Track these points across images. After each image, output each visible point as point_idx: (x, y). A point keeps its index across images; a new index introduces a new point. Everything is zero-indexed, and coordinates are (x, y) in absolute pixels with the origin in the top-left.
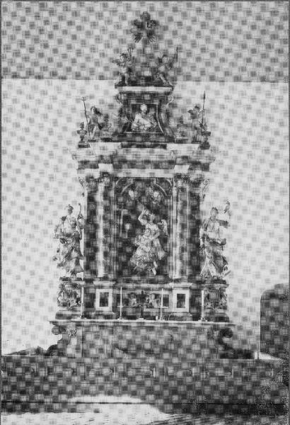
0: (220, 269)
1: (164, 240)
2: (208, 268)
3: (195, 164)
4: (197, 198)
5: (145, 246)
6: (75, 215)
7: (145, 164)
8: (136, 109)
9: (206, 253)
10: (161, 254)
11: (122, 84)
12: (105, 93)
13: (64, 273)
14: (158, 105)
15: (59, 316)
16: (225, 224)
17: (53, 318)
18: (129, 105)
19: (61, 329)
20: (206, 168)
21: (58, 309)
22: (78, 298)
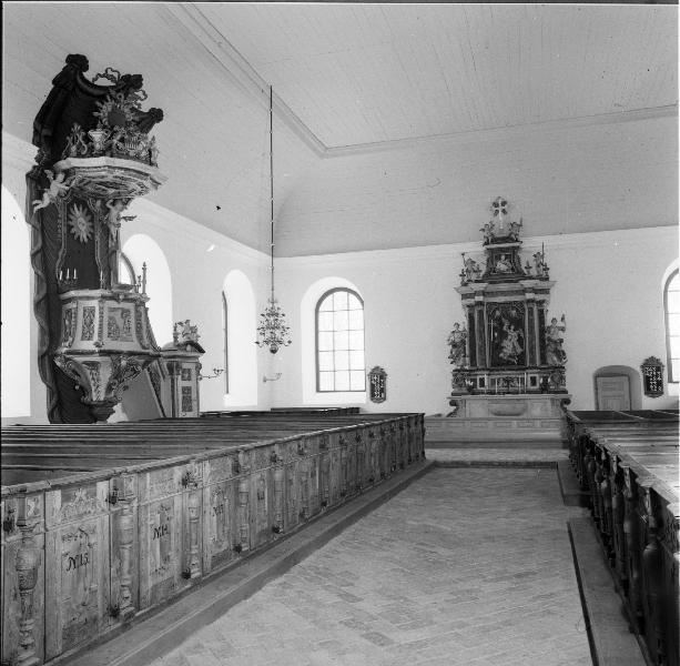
0: (560, 359)
1: (520, 341)
2: (552, 359)
3: (535, 291)
4: (541, 314)
5: (509, 346)
6: (461, 329)
7: (504, 294)
8: (499, 258)
9: (551, 347)
10: (519, 350)
11: (486, 244)
12: (477, 250)
13: (454, 367)
14: (512, 255)
15: (453, 394)
16: (563, 329)
17: (450, 395)
18: (493, 256)
19: (453, 403)
20: (546, 291)
21: (452, 390)
22: (465, 385)
